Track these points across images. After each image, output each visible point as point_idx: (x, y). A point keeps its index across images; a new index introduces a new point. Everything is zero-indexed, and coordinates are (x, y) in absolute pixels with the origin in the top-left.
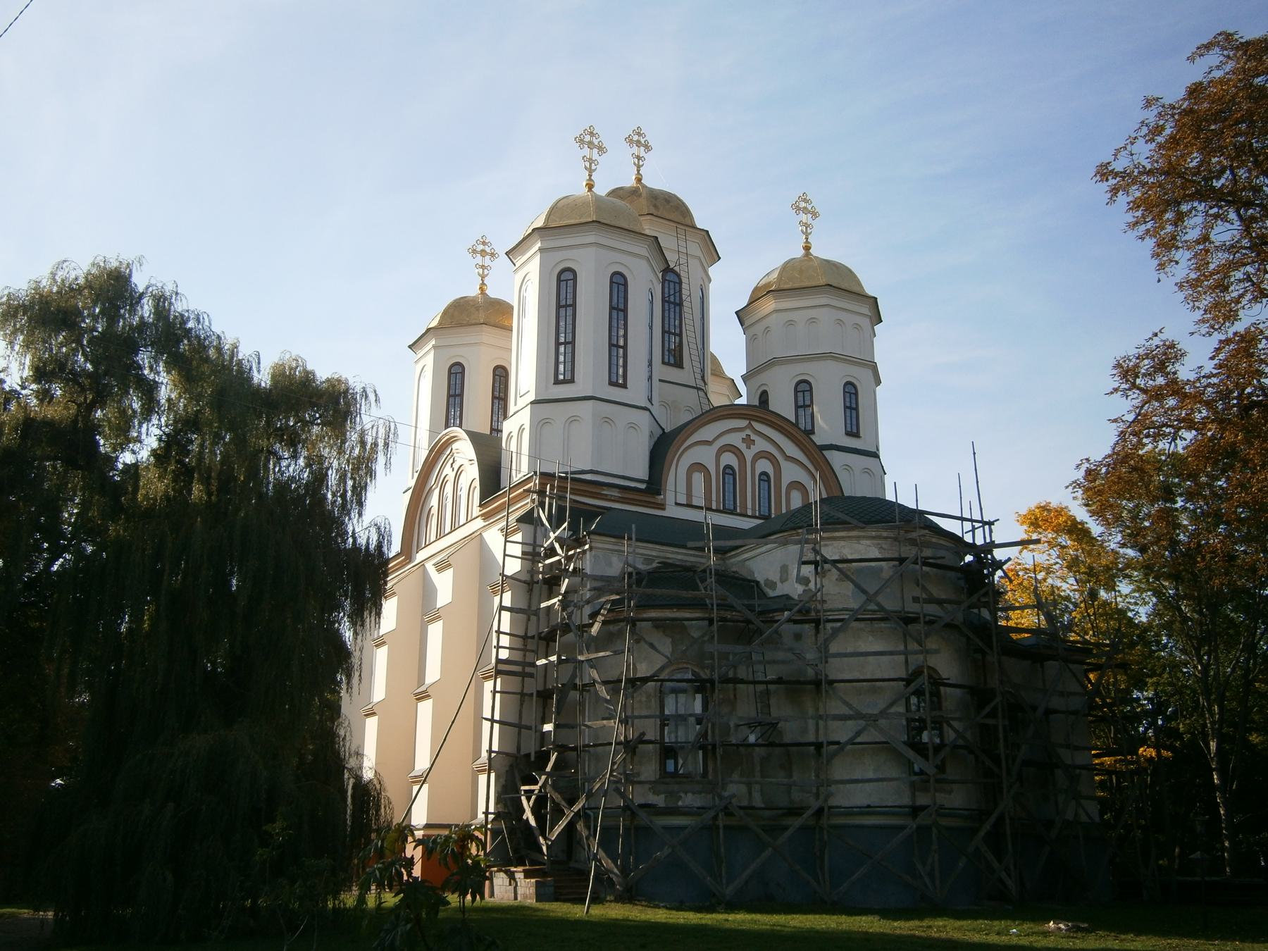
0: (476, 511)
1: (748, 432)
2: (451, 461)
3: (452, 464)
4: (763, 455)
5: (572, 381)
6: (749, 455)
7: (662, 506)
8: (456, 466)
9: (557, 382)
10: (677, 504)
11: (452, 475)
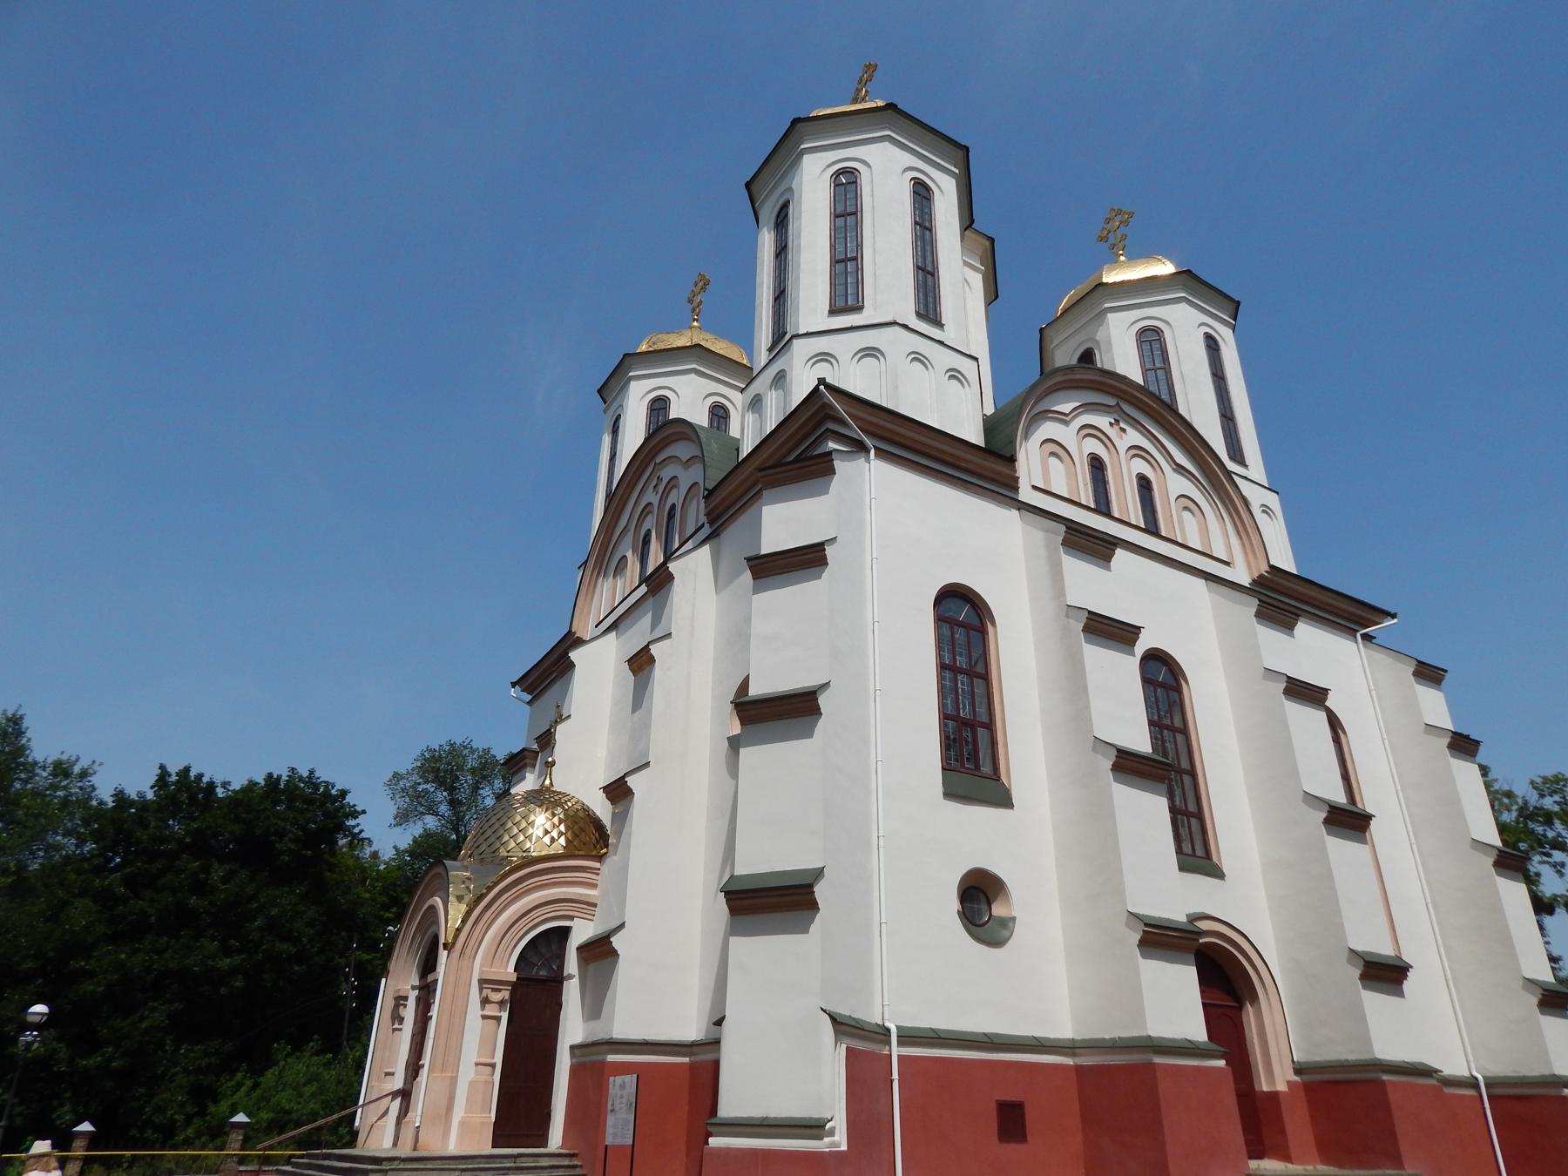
0: (703, 519)
2: (654, 483)
3: (655, 487)
5: (858, 308)
7: (1012, 484)
8: (661, 489)
9: (833, 312)
11: (656, 502)
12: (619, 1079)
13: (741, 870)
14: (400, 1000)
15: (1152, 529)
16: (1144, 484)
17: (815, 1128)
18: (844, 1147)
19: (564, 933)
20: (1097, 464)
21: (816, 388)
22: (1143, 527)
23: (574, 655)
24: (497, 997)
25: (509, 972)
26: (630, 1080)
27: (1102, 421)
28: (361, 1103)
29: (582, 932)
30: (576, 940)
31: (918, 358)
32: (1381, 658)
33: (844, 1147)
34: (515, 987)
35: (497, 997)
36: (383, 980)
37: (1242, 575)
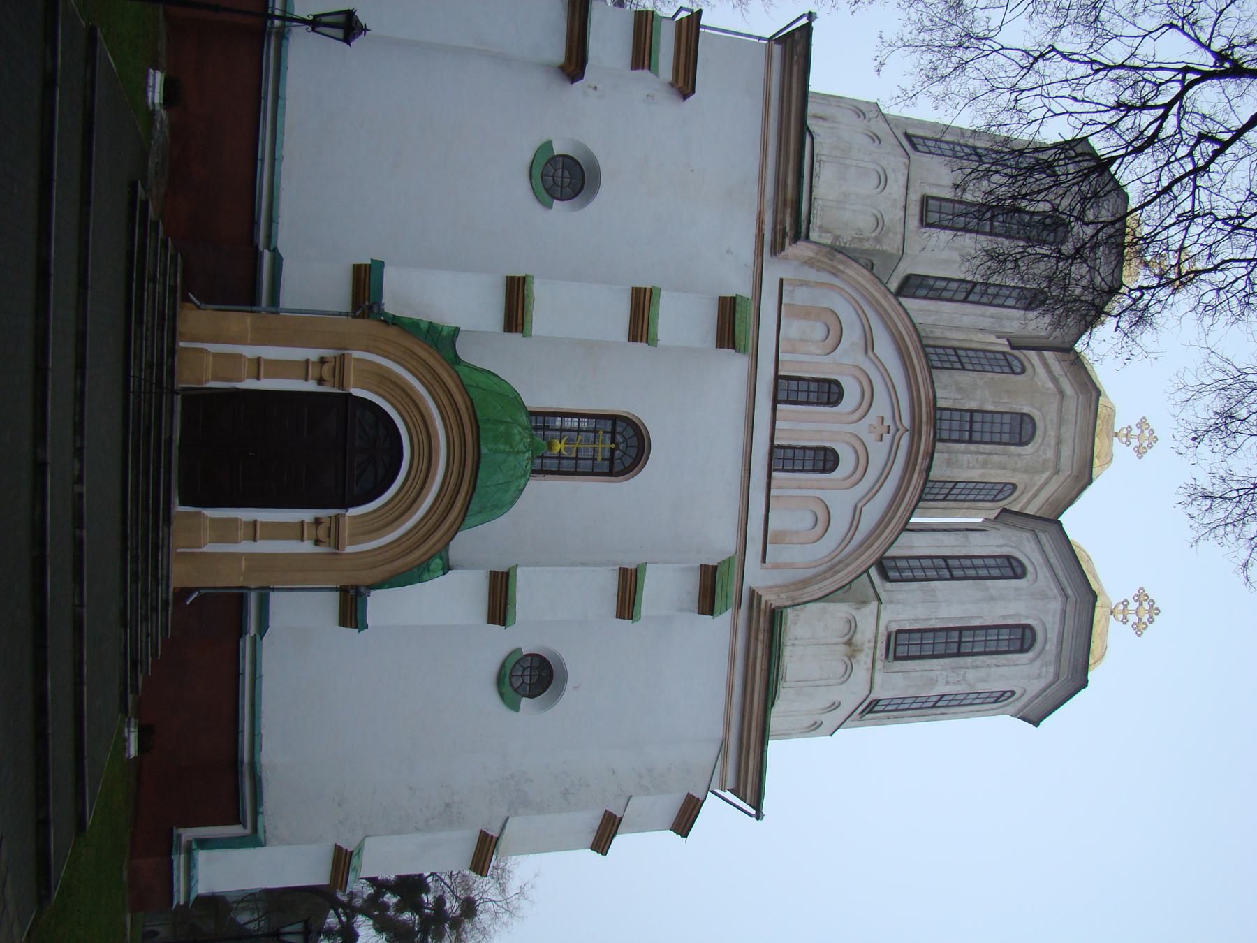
1: (892, 430)
6: (862, 428)
7: (778, 248)
10: (781, 281)
16: (825, 460)
20: (829, 393)
27: (882, 406)
37: (755, 576)
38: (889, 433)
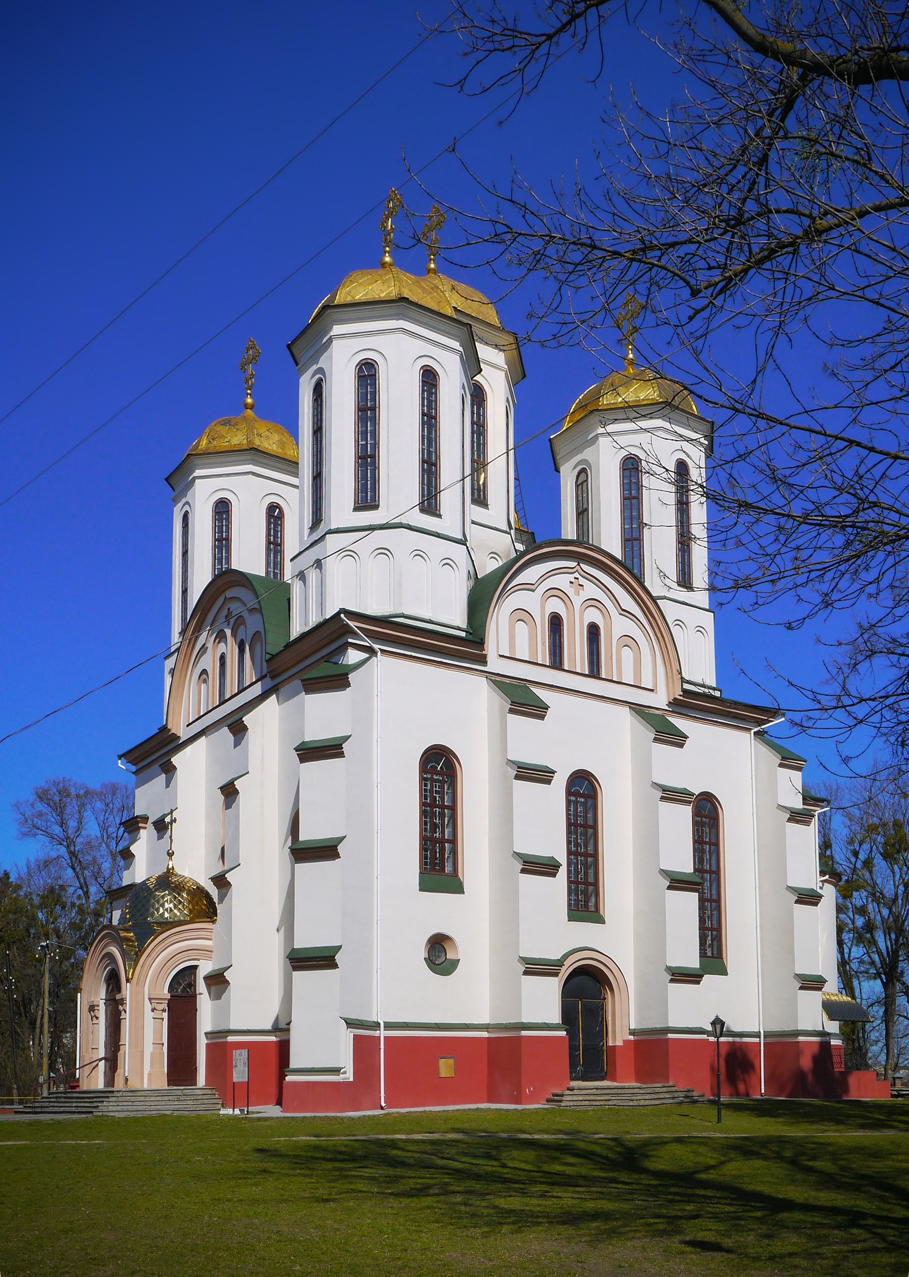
1: (577, 575)
2: (225, 612)
3: (226, 617)
4: (593, 602)
6: (578, 601)
8: (232, 621)
12: (238, 1052)
13: (297, 945)
14: (92, 1008)
15: (594, 673)
17: (336, 1071)
18: (351, 1079)
19: (195, 967)
20: (556, 622)
21: (338, 614)
22: (587, 673)
23: (175, 760)
24: (161, 1007)
25: (165, 993)
26: (245, 1053)
27: (562, 581)
28: (78, 1067)
29: (205, 968)
30: (202, 973)
31: (419, 554)
32: (764, 750)
33: (351, 1079)
34: (169, 1000)
35: (161, 1007)
36: (79, 994)
38: (577, 579)
